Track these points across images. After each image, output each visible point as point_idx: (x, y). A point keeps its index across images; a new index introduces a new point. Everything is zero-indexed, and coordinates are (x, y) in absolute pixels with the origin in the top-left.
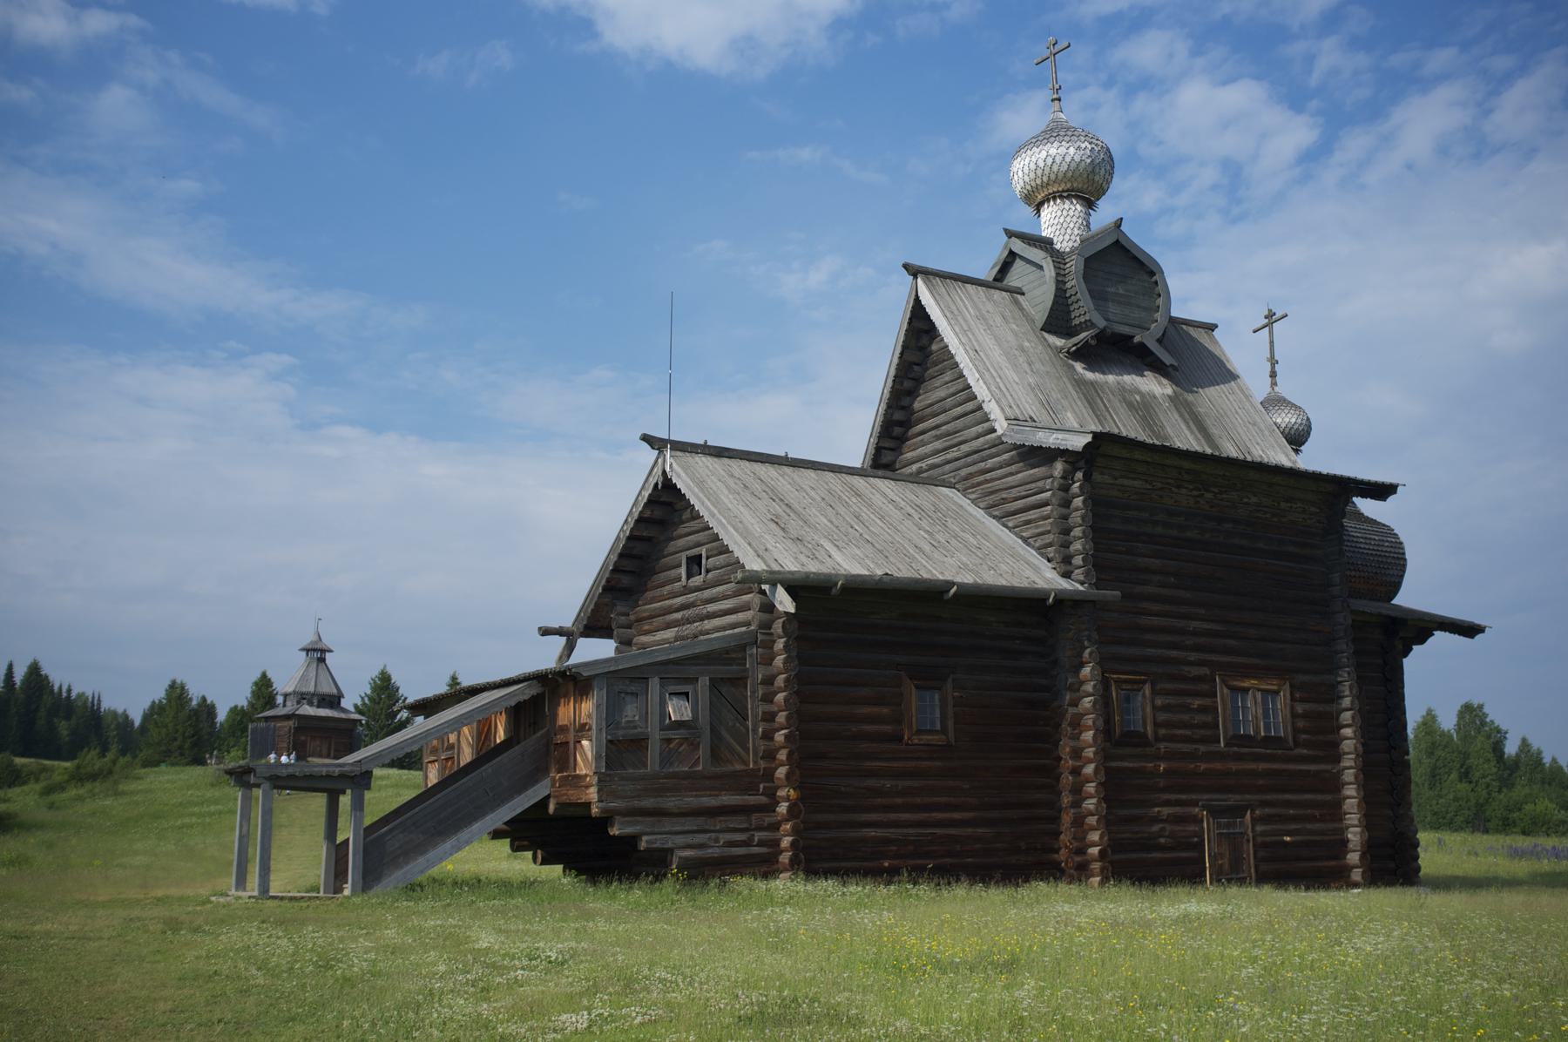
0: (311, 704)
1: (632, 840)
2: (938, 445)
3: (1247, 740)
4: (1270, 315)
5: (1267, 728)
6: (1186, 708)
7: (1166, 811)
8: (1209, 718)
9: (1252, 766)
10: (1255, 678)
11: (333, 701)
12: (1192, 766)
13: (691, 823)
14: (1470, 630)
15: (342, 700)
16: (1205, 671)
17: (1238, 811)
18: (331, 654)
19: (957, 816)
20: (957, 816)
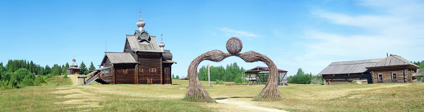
0: (74, 67)
2: (129, 49)
3: (152, 73)
5: (154, 72)
7: (144, 78)
8: (148, 71)
9: (152, 75)
11: (77, 66)
13: (107, 80)
14: (176, 63)
16: (148, 68)
17: (151, 78)
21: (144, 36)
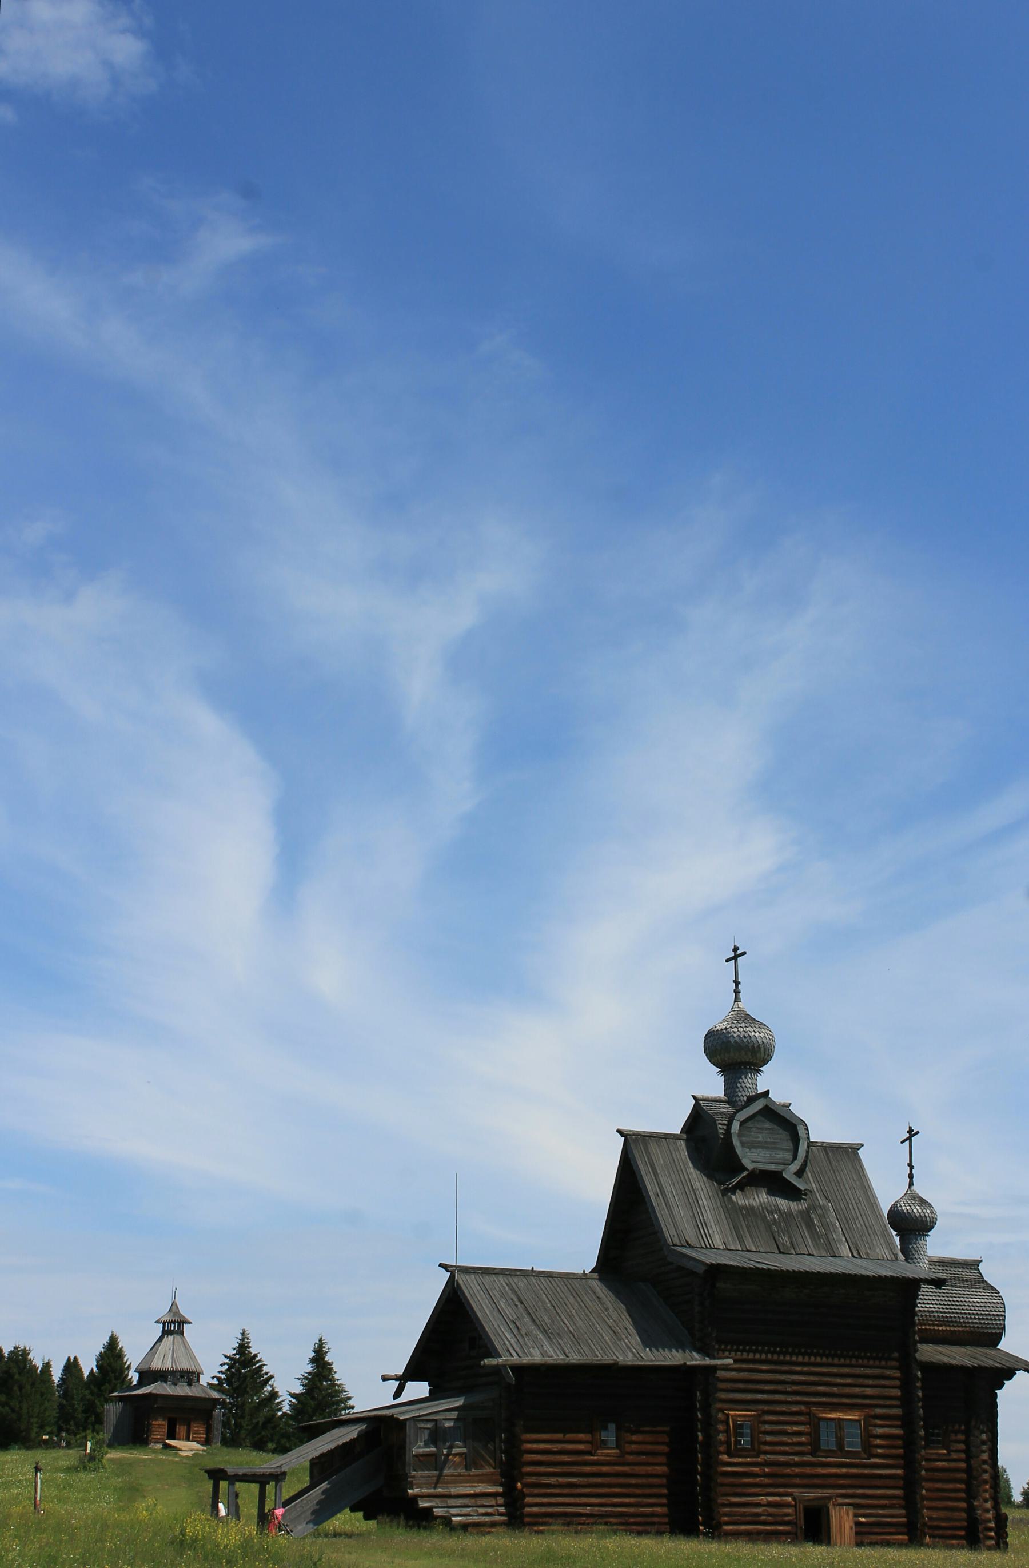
1: (429, 1510)
4: (910, 1131)
6: (785, 1433)
10: (840, 1411)
12: (789, 1470)
15: (201, 1376)
18: (189, 1325)
19: (627, 1500)
20: (627, 1500)
21: (764, 1146)
